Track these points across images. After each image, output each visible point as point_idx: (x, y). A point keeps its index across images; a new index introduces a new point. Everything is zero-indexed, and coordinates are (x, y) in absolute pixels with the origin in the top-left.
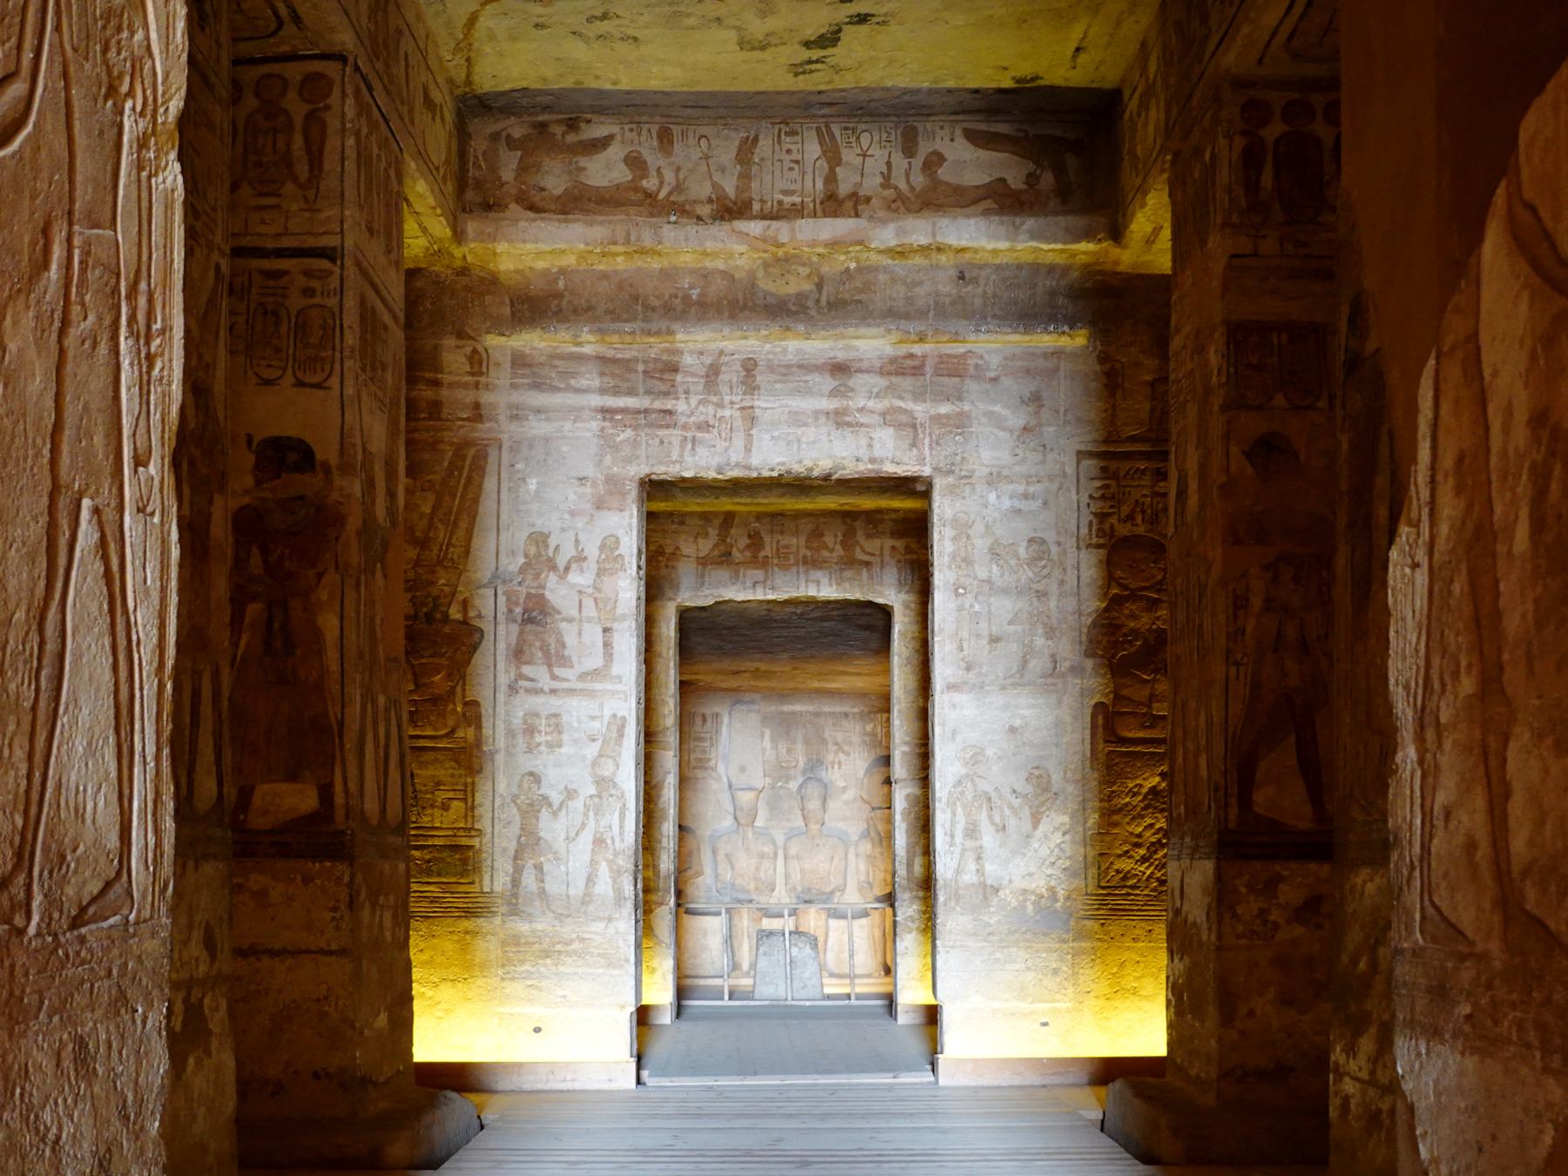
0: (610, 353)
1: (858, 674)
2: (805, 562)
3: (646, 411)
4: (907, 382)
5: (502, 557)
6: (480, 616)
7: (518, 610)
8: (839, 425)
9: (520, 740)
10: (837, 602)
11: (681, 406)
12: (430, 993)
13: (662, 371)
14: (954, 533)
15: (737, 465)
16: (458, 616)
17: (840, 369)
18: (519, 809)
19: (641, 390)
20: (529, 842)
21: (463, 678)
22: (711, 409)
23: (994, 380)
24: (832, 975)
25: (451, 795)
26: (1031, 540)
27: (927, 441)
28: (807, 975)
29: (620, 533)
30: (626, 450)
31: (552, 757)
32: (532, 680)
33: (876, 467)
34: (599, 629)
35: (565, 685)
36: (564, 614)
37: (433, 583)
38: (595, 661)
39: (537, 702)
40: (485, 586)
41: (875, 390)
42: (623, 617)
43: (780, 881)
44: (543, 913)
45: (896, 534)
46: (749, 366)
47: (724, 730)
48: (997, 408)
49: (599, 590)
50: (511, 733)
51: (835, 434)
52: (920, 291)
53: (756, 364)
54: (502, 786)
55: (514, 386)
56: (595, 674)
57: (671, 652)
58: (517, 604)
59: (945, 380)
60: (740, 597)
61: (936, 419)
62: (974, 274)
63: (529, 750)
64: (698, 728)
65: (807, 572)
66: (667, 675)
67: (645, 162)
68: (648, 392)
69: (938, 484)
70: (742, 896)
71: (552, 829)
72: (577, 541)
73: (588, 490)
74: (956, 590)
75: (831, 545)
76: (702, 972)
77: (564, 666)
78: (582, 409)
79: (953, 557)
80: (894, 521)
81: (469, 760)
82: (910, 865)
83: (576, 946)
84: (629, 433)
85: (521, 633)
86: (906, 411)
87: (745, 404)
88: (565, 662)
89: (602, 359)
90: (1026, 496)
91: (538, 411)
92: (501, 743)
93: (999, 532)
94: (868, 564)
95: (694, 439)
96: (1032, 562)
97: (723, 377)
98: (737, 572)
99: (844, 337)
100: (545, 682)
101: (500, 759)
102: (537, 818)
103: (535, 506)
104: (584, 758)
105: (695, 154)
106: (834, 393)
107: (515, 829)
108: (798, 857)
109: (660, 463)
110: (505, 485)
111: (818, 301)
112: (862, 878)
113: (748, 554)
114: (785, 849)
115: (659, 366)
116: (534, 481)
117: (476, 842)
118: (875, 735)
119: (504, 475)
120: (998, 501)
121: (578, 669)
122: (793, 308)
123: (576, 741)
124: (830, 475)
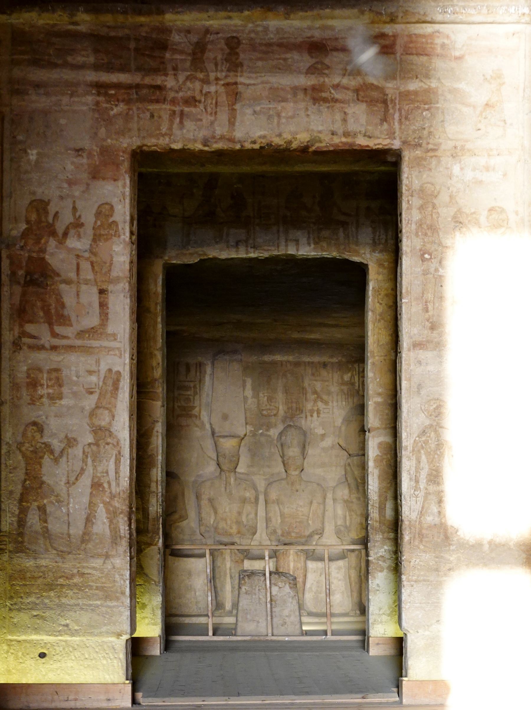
1: (336, 326)
3: (138, 86)
7: (21, 273)
8: (315, 100)
9: (24, 392)
10: (315, 260)
11: (170, 82)
15: (222, 138)
18: (24, 455)
19: (133, 67)
24: (310, 614)
28: (286, 612)
29: (114, 201)
31: (53, 408)
32: (34, 337)
34: (95, 290)
35: (65, 342)
38: (92, 320)
39: (39, 357)
42: (118, 280)
43: (261, 525)
44: (47, 550)
46: (233, 44)
47: (207, 378)
50: (16, 387)
51: (313, 109)
53: (239, 43)
56: (92, 332)
57: (159, 308)
60: (224, 255)
63: (33, 402)
66: (155, 329)
68: (139, 69)
70: (225, 540)
71: (54, 474)
72: (75, 209)
76: (186, 611)
82: (382, 509)
84: (121, 107)
85: (24, 294)
88: (64, 320)
95: (182, 113)
97: (210, 55)
100: (46, 339)
102: (40, 464)
104: (83, 409)
107: (21, 474)
108: (278, 502)
109: (151, 136)
112: (339, 522)
114: (266, 494)
118: (353, 384)
121: (77, 327)
123: (75, 394)
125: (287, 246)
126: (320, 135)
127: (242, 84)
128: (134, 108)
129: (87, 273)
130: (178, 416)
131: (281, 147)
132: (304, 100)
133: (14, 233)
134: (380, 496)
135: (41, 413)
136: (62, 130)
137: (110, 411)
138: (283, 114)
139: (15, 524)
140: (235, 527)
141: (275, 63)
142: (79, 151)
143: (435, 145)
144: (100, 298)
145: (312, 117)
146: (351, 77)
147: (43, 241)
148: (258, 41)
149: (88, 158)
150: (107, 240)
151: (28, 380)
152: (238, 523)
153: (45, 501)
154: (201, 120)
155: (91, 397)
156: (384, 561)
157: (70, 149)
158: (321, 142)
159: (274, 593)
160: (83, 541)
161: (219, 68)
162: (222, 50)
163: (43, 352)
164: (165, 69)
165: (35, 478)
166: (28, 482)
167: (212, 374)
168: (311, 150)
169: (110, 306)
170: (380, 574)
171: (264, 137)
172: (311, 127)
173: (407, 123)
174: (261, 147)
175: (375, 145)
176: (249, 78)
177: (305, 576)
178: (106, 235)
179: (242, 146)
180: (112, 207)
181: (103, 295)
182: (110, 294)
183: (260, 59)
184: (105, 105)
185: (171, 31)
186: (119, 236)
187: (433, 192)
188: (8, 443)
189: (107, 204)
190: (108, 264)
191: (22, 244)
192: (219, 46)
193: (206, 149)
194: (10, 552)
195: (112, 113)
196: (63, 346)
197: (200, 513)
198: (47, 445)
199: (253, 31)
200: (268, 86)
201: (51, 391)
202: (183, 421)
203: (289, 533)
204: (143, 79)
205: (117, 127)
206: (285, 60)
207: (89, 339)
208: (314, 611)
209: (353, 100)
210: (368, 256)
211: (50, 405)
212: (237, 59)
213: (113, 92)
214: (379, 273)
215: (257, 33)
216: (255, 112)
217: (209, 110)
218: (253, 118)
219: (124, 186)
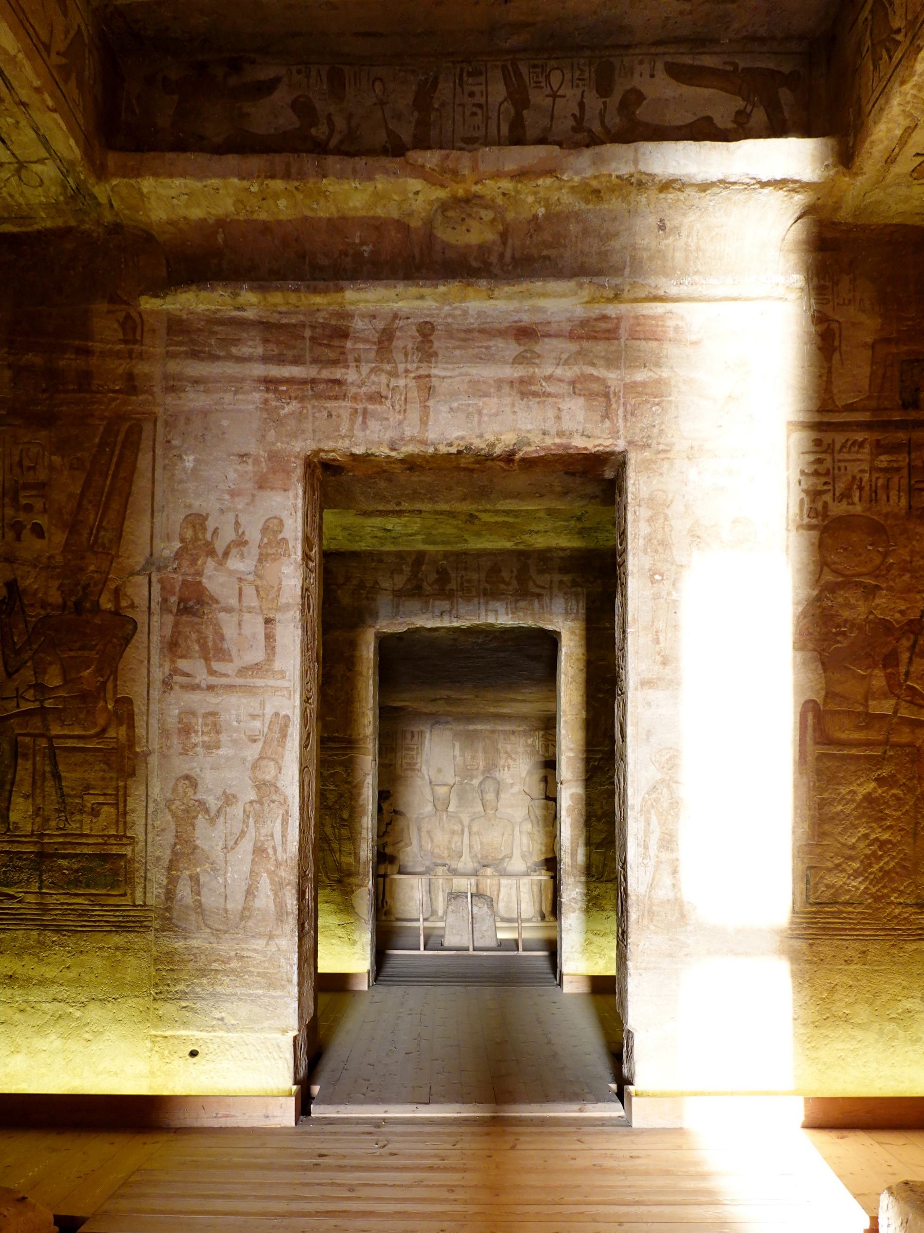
1: (524, 701)
2: (485, 595)
3: (313, 381)
5: (157, 541)
6: (132, 606)
7: (173, 599)
8: (523, 395)
9: (175, 740)
10: (512, 630)
11: (351, 375)
12: (78, 1014)
15: (412, 439)
16: (109, 606)
17: (525, 333)
18: (174, 815)
19: (308, 359)
20: (184, 851)
21: (115, 672)
22: (384, 378)
24: (503, 920)
25: (101, 799)
27: (621, 412)
28: (485, 928)
29: (284, 515)
30: (292, 424)
31: (209, 759)
33: (564, 441)
34: (260, 620)
35: (224, 681)
36: (223, 604)
37: (82, 569)
38: (257, 655)
40: (138, 573)
41: (564, 356)
42: (287, 607)
43: (466, 850)
44: (199, 928)
45: (563, 570)
46: (426, 331)
47: (427, 742)
49: (260, 577)
50: (165, 733)
51: (520, 404)
53: (433, 328)
54: (155, 791)
56: (255, 669)
57: (371, 672)
60: (429, 625)
63: (185, 752)
64: (408, 741)
65: (487, 603)
66: (367, 691)
68: (315, 361)
70: (439, 861)
71: (209, 837)
72: (237, 523)
73: (250, 468)
75: (507, 579)
76: (409, 916)
77: (224, 660)
78: (243, 380)
80: (561, 558)
81: (123, 763)
82: (573, 855)
83: (234, 964)
84: (294, 405)
85: (176, 625)
86: (598, 379)
87: (422, 372)
88: (223, 654)
91: (196, 382)
92: (155, 745)
94: (539, 596)
95: (365, 412)
97: (398, 343)
98: (427, 602)
101: (154, 760)
102: (193, 825)
103: (191, 486)
104: (244, 760)
106: (519, 360)
107: (169, 838)
108: (478, 833)
109: (328, 438)
110: (160, 463)
112: (524, 849)
113: (436, 587)
114: (470, 827)
116: (191, 458)
117: (127, 851)
118: (534, 746)
119: (159, 451)
121: (238, 663)
122: (475, 264)
123: (235, 742)
124: (512, 453)
125: (486, 615)
126: (529, 436)
127: (436, 376)
128: (309, 407)
129: (251, 598)
130: (406, 769)
131: (483, 452)
132: (510, 395)
133: (166, 553)
134: (572, 843)
135: (195, 764)
136: (224, 433)
137: (277, 762)
138: (485, 411)
139: (163, 897)
140: (446, 852)
141: (476, 351)
142: (243, 456)
144: (266, 628)
145: (520, 414)
147: (199, 562)
148: (456, 326)
149: (254, 464)
150: (275, 560)
151: (180, 726)
152: (449, 849)
153: (198, 870)
154: (387, 419)
155: (254, 745)
156: (576, 903)
157: (233, 455)
158: (529, 444)
159: (474, 912)
160: (242, 918)
161: (409, 358)
162: (413, 337)
164: (346, 361)
165: (186, 842)
166: (178, 847)
167: (430, 739)
169: (278, 638)
170: (572, 915)
171: (462, 438)
172: (519, 426)
174: (459, 452)
177: (499, 890)
179: (436, 450)
181: (270, 625)
183: (458, 347)
184: (274, 403)
185: (352, 317)
186: (289, 555)
188: (155, 800)
189: (275, 518)
190: (275, 589)
191: (175, 566)
192: (409, 333)
193: (393, 454)
194: (156, 930)
195: (282, 412)
197: (420, 841)
198: (201, 803)
199: (450, 315)
200: (467, 379)
201: (206, 739)
202: (409, 773)
203: (487, 857)
204: (319, 373)
205: (289, 428)
206: (487, 348)
207: (252, 676)
208: (506, 916)
210: (561, 624)
211: (204, 756)
212: (430, 348)
213: (284, 388)
214: (571, 640)
215: (454, 317)
216: (451, 409)
217: (397, 407)
218: (449, 416)
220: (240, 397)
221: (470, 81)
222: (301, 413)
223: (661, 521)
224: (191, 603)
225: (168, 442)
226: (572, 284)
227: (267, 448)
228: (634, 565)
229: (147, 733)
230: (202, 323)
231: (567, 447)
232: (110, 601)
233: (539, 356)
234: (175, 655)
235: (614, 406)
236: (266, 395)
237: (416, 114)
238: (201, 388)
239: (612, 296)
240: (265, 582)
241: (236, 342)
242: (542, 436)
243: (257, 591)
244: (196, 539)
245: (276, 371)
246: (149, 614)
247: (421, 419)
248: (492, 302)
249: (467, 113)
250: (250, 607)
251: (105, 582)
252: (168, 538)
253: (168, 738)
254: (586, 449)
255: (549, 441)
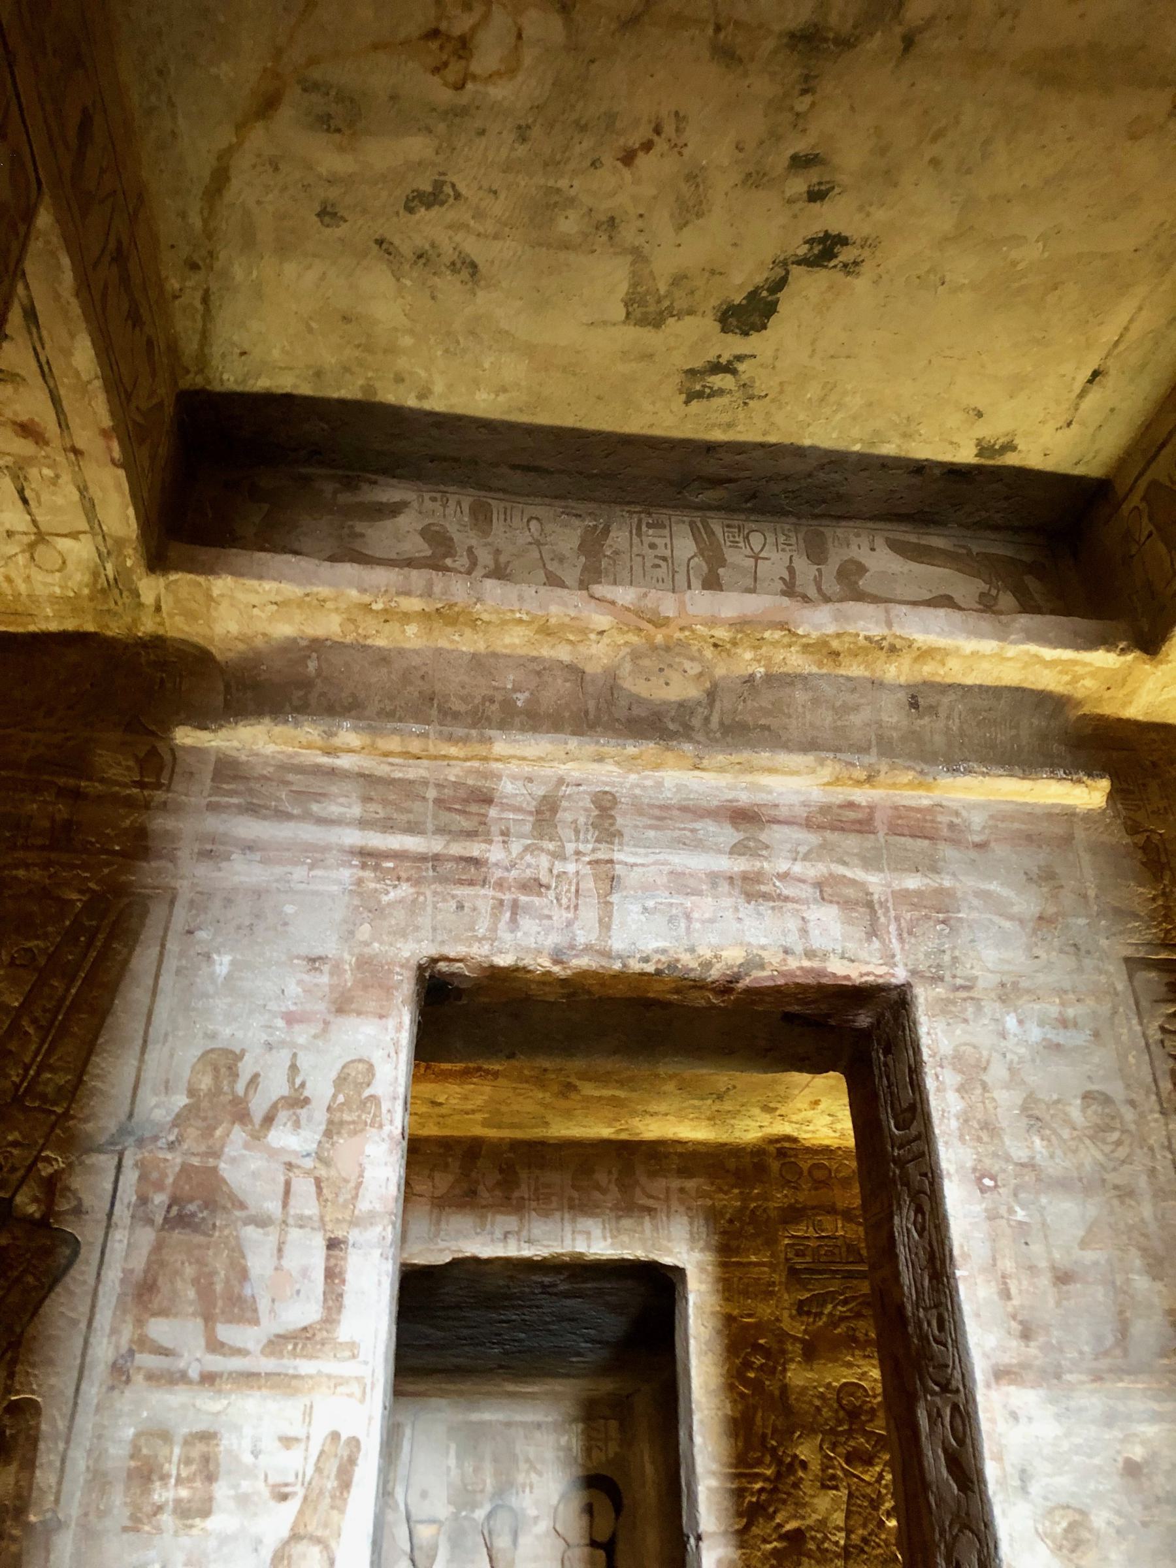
0: (382, 769)
3: (436, 858)
4: (851, 842)
5: (145, 1092)
7: (160, 1199)
8: (749, 896)
11: (495, 854)
13: (466, 801)
14: (959, 1078)
15: (588, 949)
16: (32, 1209)
17: (745, 817)
19: (430, 827)
22: (544, 861)
23: (981, 846)
26: (1087, 1096)
27: (893, 928)
29: (377, 1057)
31: (185, 1541)
34: (318, 1242)
38: (304, 1311)
40: (100, 1150)
41: (803, 849)
42: (371, 1218)
46: (605, 807)
48: (994, 886)
49: (326, 1162)
51: (747, 909)
52: (857, 719)
53: (614, 800)
55: (213, 808)
56: (303, 1339)
58: (159, 1186)
59: (908, 842)
61: (903, 896)
62: (932, 701)
63: (134, 1526)
67: (451, 539)
68: (440, 831)
69: (923, 997)
74: (980, 1177)
78: (326, 848)
79: (965, 1119)
85: (158, 1247)
86: (853, 882)
87: (600, 855)
88: (241, 1309)
89: (367, 778)
90: (1064, 1023)
91: (249, 847)
93: (1033, 1078)
95: (515, 905)
96: (1099, 1131)
97: (565, 816)
99: (751, 770)
100: (195, 1358)
103: (221, 1004)
104: (257, 1544)
105: (523, 538)
106: (737, 850)
109: (457, 939)
111: (707, 720)
115: (462, 793)
116: (227, 959)
120: (1019, 1031)
122: (671, 726)
123: (243, 1501)
126: (764, 954)
127: (620, 863)
128: (428, 893)
129: (305, 1202)
131: (692, 975)
132: (730, 895)
136: (286, 924)
137: (327, 1547)
138: (695, 915)
141: (677, 833)
143: (966, 979)
144: (328, 1258)
145: (747, 922)
146: (807, 864)
147: (218, 1133)
149: (331, 974)
150: (355, 1133)
151: (133, 1464)
154: (549, 917)
155: (284, 1506)
157: (298, 957)
158: (762, 967)
161: (582, 837)
162: (586, 810)
163: (181, 1387)
164: (488, 833)
168: (741, 985)
169: (349, 1277)
171: (664, 951)
173: (913, 940)
174: (658, 972)
175: (862, 975)
176: (636, 854)
178: (354, 1122)
179: (624, 966)
180: (371, 1069)
181: (336, 1252)
182: (350, 1250)
183: (651, 827)
184: (372, 885)
185: (499, 777)
186: (381, 1126)
187: (979, 1060)
189: (360, 1061)
190: (352, 1184)
191: (172, 1138)
192: (581, 804)
193: (556, 969)
195: (385, 899)
196: (230, 1374)
199: (638, 786)
200: (667, 868)
201: (184, 1493)
204: (446, 846)
205: (393, 922)
206: (693, 831)
207: (294, 1354)
209: (815, 899)
212: (612, 825)
213: (391, 865)
215: (644, 788)
216: (645, 909)
217: (564, 901)
218: (643, 918)
219: (399, 1029)
220: (317, 872)
221: (651, 532)
222: (414, 901)
223: (979, 1091)
224: (192, 1207)
225: (190, 932)
226: (809, 759)
227: (356, 951)
228: (949, 1161)
229: (60, 1483)
230: (271, 769)
231: (821, 973)
232: (35, 1200)
233: (767, 847)
234: (146, 1308)
235: (882, 920)
236: (361, 873)
237: (583, 559)
238: (258, 856)
239: (863, 775)
240: (333, 1173)
241: (319, 797)
242: (781, 955)
243: (319, 1188)
244: (216, 1092)
245: (378, 841)
246: (109, 1226)
247: (600, 921)
248: (697, 773)
249: (648, 564)
250: (301, 1217)
251: (34, 1163)
252: (166, 1088)
253: (103, 1492)
254: (847, 977)
255: (793, 964)
